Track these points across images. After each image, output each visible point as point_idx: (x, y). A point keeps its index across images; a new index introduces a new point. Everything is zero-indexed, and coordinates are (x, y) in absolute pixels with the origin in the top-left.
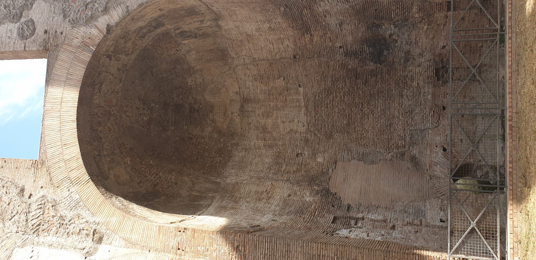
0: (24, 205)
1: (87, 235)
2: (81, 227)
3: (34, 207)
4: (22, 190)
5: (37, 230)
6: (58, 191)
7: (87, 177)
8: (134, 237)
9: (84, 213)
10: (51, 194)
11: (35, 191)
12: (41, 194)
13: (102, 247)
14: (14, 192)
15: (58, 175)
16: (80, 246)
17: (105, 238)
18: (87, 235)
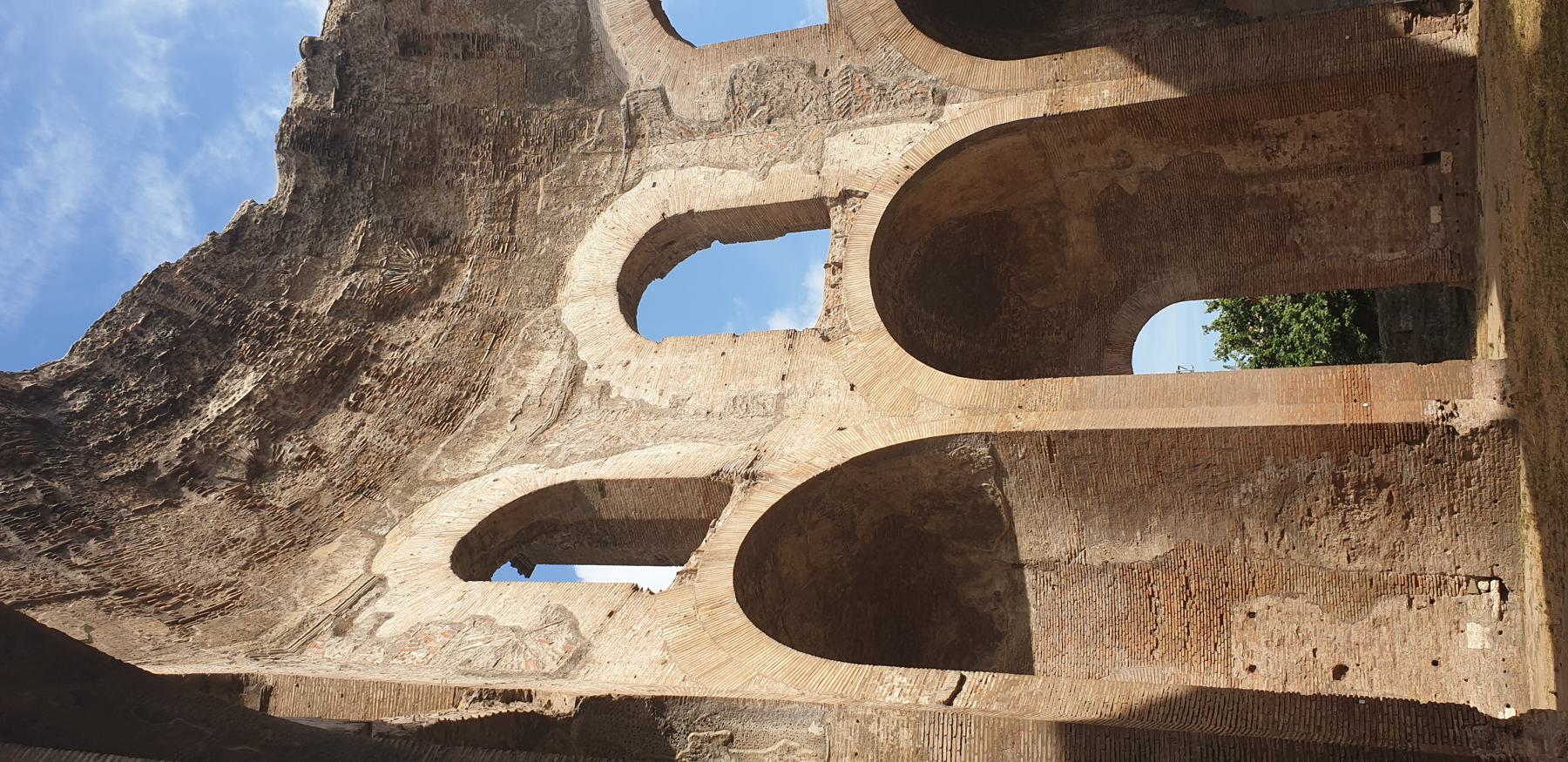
0: (819, 87)
1: (924, 99)
2: (913, 91)
3: (836, 84)
4: (813, 67)
5: (846, 112)
6: (869, 55)
7: (910, 26)
8: (991, 85)
9: (915, 74)
10: (857, 62)
11: (833, 64)
12: (843, 65)
13: (947, 107)
14: (800, 73)
15: (863, 34)
16: (918, 112)
17: (949, 97)
18: (924, 99)
